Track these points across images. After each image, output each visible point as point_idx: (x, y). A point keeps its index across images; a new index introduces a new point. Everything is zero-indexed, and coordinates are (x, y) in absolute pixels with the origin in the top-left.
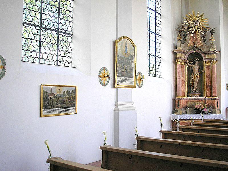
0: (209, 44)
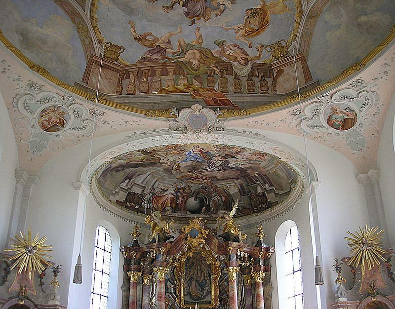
0: (48, 292)
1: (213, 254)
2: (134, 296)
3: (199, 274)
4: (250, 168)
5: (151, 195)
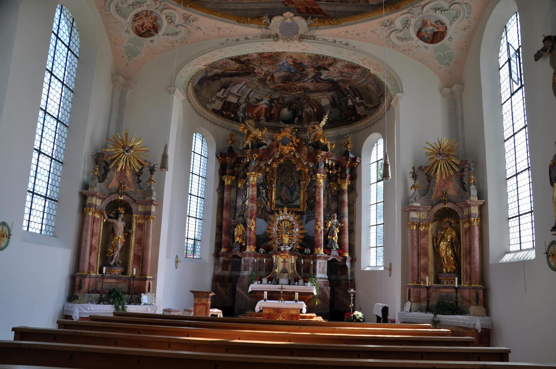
1: (303, 160)
2: (228, 198)
3: (290, 181)
4: (340, 81)
5: (246, 104)
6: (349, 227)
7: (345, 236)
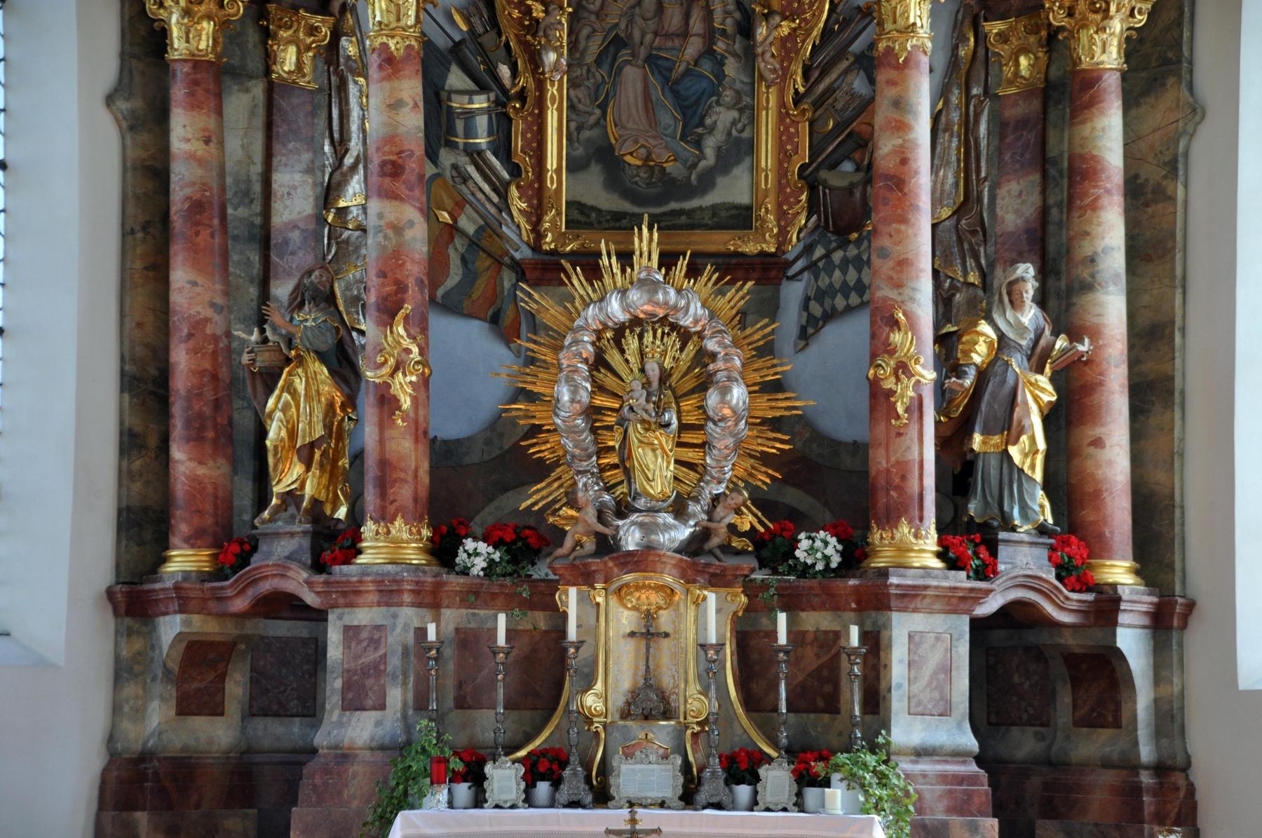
2: (200, 162)
3: (673, 18)
6: (1134, 363)
7: (1098, 431)
